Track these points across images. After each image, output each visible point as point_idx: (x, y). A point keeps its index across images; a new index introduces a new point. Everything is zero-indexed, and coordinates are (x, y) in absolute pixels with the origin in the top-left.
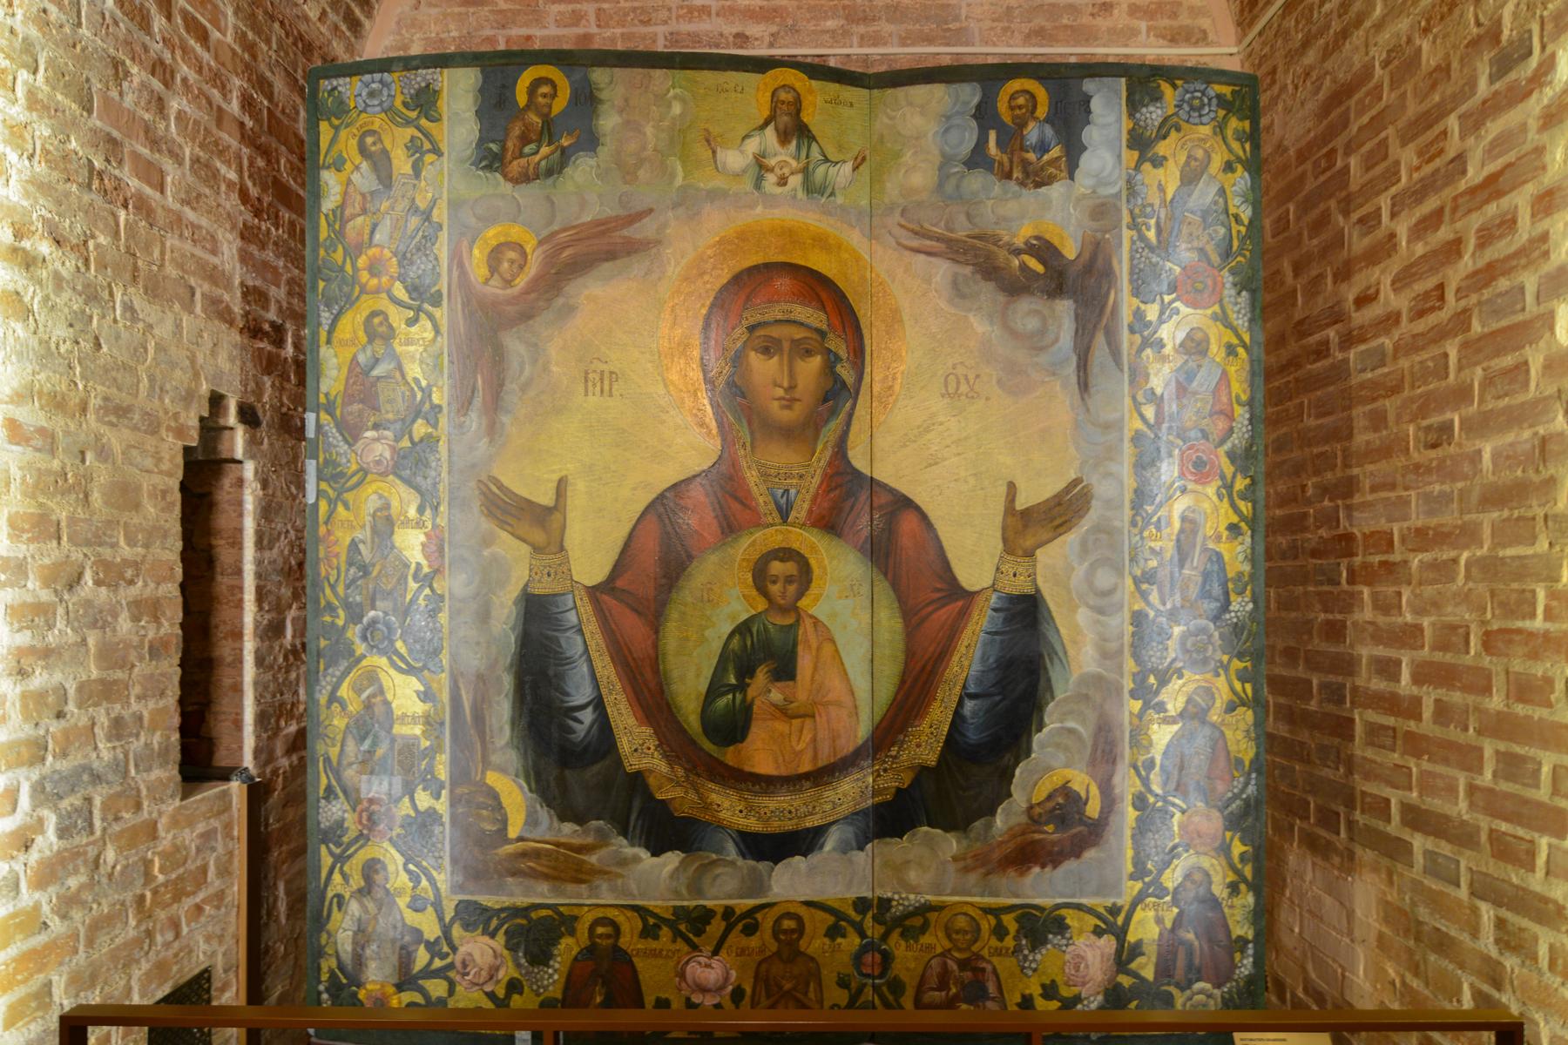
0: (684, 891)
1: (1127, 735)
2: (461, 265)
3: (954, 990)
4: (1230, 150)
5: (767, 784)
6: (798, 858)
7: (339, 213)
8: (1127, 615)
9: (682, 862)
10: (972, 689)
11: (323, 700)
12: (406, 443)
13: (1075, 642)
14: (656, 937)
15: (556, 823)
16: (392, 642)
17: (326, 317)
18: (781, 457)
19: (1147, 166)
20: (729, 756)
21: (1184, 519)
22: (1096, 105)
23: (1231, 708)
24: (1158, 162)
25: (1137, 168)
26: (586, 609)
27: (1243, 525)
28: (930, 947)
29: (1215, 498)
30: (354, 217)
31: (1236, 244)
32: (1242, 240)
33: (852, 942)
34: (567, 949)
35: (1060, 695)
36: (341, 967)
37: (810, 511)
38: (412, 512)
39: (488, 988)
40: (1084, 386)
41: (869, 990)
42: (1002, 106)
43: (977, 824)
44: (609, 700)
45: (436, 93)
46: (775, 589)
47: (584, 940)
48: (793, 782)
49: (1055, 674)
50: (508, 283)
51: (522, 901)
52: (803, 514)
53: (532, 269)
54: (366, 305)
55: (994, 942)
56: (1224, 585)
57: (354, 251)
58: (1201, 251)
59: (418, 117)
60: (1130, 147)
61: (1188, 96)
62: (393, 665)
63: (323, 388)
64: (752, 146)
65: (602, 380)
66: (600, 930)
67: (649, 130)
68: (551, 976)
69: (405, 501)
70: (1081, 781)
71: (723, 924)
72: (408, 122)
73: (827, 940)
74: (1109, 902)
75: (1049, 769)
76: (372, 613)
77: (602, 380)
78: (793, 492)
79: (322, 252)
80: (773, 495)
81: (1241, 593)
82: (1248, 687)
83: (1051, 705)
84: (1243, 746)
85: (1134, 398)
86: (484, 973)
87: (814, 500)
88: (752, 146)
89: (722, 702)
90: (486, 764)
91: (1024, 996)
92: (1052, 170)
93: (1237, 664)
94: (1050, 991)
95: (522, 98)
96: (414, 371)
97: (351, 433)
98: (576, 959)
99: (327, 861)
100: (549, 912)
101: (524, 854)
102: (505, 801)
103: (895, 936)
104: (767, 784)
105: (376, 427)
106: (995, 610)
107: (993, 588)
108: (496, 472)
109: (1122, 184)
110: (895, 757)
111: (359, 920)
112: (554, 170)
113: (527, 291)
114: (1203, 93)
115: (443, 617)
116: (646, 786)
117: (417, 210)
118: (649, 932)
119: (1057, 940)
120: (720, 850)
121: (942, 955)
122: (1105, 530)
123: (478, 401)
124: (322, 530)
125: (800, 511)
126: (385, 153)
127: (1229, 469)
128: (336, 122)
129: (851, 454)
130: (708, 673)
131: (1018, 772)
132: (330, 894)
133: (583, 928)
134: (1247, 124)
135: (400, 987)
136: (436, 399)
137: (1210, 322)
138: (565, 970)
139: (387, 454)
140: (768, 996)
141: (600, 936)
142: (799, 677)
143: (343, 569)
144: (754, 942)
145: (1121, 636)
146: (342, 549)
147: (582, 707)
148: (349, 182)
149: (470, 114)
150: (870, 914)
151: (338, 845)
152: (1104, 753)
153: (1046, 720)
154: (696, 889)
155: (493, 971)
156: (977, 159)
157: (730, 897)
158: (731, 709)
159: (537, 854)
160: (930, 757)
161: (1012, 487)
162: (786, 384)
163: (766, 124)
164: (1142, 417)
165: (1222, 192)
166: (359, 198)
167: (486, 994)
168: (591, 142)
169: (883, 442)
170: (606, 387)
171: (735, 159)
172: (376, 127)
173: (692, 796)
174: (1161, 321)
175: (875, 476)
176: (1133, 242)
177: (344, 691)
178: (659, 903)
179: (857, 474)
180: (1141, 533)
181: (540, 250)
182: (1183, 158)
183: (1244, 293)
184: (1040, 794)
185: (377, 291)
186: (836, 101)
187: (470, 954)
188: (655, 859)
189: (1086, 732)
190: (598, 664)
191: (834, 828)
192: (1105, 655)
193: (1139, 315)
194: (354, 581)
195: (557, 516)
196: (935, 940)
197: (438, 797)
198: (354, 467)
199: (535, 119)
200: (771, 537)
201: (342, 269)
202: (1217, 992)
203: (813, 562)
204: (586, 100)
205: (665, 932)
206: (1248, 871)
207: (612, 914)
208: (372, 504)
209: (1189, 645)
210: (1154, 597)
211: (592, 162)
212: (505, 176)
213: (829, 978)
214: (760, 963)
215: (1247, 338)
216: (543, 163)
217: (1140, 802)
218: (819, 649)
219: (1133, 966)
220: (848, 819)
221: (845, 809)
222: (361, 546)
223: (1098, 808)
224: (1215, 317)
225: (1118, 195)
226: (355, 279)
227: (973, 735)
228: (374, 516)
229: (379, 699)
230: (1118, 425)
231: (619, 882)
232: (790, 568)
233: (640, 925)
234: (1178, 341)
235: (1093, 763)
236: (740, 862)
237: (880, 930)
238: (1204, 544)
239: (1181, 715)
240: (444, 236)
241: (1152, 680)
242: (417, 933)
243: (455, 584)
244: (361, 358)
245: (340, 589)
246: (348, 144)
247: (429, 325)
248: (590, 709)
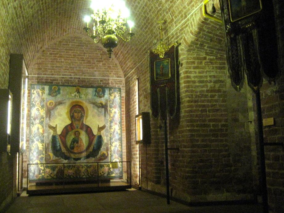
5: (75, 153)
8: (109, 137)
11: (31, 146)
16: (39, 140)
18: (77, 122)
20: (72, 151)
22: (106, 91)
23: (119, 146)
24: (112, 96)
26: (59, 137)
32: (120, 103)
33: (84, 169)
34: (57, 169)
38: (41, 128)
40: (105, 116)
44: (61, 145)
47: (58, 168)
49: (103, 143)
50: (51, 106)
53: (54, 105)
54: (36, 107)
57: (35, 102)
60: (109, 94)
63: (32, 115)
64: (75, 94)
67: (65, 92)
69: (40, 126)
70: (105, 152)
72: (41, 90)
88: (75, 94)
90: (49, 152)
93: (119, 142)
94: (103, 172)
96: (41, 114)
97: (35, 119)
102: (51, 156)
104: (75, 153)
107: (97, 135)
108: (50, 124)
112: (56, 95)
113: (53, 107)
115: (44, 138)
122: (107, 129)
123: (48, 117)
125: (79, 128)
130: (70, 143)
135: (39, 175)
136: (44, 116)
144: (75, 169)
152: (107, 150)
155: (49, 172)
156: (95, 95)
161: (99, 126)
168: (59, 93)
171: (73, 95)
177: (33, 145)
179: (84, 124)
184: (102, 153)
188: (65, 161)
189: (105, 148)
192: (107, 141)
193: (110, 110)
196: (92, 168)
197: (43, 155)
200: (77, 130)
204: (59, 89)
205: (66, 168)
210: (112, 136)
212: (52, 96)
213: (82, 172)
217: (111, 154)
220: (84, 157)
230: (108, 120)
232: (78, 133)
239: (114, 146)
240: (45, 101)
242: (41, 169)
243: (46, 134)
246: (35, 92)
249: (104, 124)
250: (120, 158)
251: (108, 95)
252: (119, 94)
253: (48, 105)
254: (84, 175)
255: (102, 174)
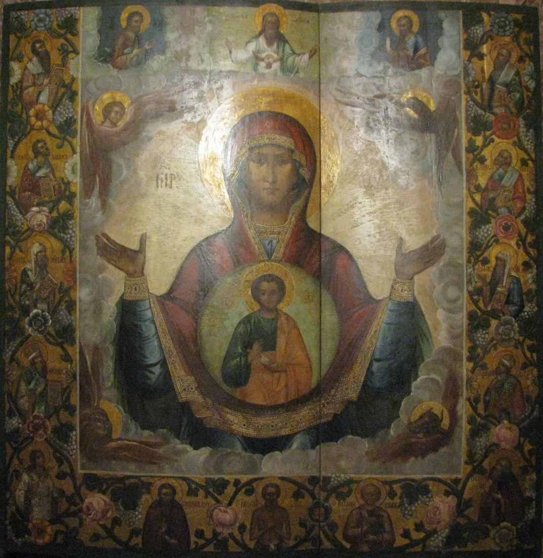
0: (211, 469)
1: (464, 383)
2: (88, 114)
3: (365, 528)
4: (522, 50)
5: (259, 410)
6: (277, 453)
7: (20, 85)
9: (211, 454)
10: (377, 356)
12: (55, 214)
13: (436, 329)
14: (196, 495)
15: (139, 430)
17: (11, 143)
19: (475, 60)
20: (237, 393)
21: (497, 258)
22: (445, 25)
23: (525, 366)
25: (469, 60)
26: (156, 309)
27: (531, 262)
28: (352, 504)
29: (515, 247)
30: (27, 87)
31: (526, 102)
33: (307, 501)
34: (146, 500)
35: (427, 360)
36: (18, 509)
37: (284, 253)
39: (101, 522)
41: (317, 528)
42: (394, 25)
43: (380, 433)
45: (76, 20)
46: (264, 298)
47: (156, 497)
48: (274, 409)
49: (424, 347)
50: (114, 124)
51: (120, 474)
52: (280, 255)
54: (35, 136)
55: (388, 500)
56: (521, 294)
58: (507, 106)
59: (66, 33)
60: (465, 48)
61: (497, 20)
62: (48, 341)
64: (252, 47)
65: (166, 179)
66: (164, 491)
68: (137, 516)
70: (438, 407)
71: (234, 489)
73: (293, 499)
74: (454, 476)
75: (420, 401)
76: (35, 311)
77: (166, 179)
78: (274, 242)
79: (9, 107)
80: (263, 244)
81: (530, 302)
82: (534, 355)
83: (422, 365)
84: (531, 388)
85: (469, 189)
86: (99, 514)
87: (286, 247)
88: (252, 47)
89: (234, 362)
91: (404, 530)
92: (422, 61)
93: (528, 342)
95: (124, 24)
97: (24, 209)
98: (151, 507)
99: (9, 450)
100: (136, 481)
101: (120, 448)
103: (332, 498)
104: (259, 410)
105: (38, 205)
106: (391, 311)
107: (390, 298)
108: (107, 232)
109: (460, 69)
110: (334, 396)
111: (28, 484)
114: (506, 18)
116: (189, 409)
117: (64, 86)
118: (192, 492)
119: (425, 498)
120: (232, 446)
121: (359, 508)
124: (7, 263)
125: (279, 254)
126: (47, 54)
127: (523, 230)
128: (19, 35)
129: (308, 220)
130: (225, 347)
131: (403, 404)
132: (11, 470)
133: (155, 490)
134: (531, 35)
137: (511, 147)
138: (145, 513)
139: (45, 220)
140: (260, 529)
141: (165, 494)
142: (277, 349)
143: (18, 286)
145: (462, 327)
146: (18, 275)
147: (154, 365)
148: (26, 68)
149: (95, 32)
150: (318, 486)
151: (15, 443)
153: (419, 373)
154: (218, 469)
155: (105, 512)
157: (239, 473)
158: (238, 366)
159: (128, 448)
160: (353, 395)
162: (270, 180)
163: (260, 34)
164: (473, 199)
165: (517, 74)
166: (31, 76)
167: (101, 525)
169: (327, 212)
170: (169, 182)
172: (42, 38)
173: (217, 416)
174: (485, 146)
175: (323, 232)
176: (467, 102)
178: (198, 476)
180: (473, 266)
181: (132, 107)
182: (495, 54)
183: (531, 130)
184: (415, 416)
185: (42, 128)
186: (300, 20)
187: (91, 503)
188: (196, 451)
190: (163, 341)
191: (298, 436)
194: (25, 292)
195: (141, 256)
196: (354, 499)
198: (26, 228)
199: (131, 35)
201: (20, 116)
202: (514, 528)
203: (286, 283)
205: (201, 493)
206: (534, 460)
207: (173, 482)
208: (36, 248)
209: (500, 331)
211: (163, 58)
214: (255, 511)
215: (533, 156)
216: (135, 58)
218: (289, 333)
219: (466, 513)
220: (307, 431)
221: (303, 425)
222: (29, 273)
223: (448, 424)
224: (514, 144)
225: (458, 76)
226: (28, 122)
227: (377, 383)
228: (36, 255)
229: (39, 359)
231: (176, 464)
232: (273, 285)
233: (187, 488)
234: (494, 157)
235: (445, 398)
236: (244, 454)
237: (323, 495)
238: (509, 273)
240: (79, 98)
241: (479, 350)
244: (31, 166)
245: (17, 297)
247: (69, 147)
248: (158, 366)
249: (434, 233)
250: (531, 443)
251: (459, 53)
252: (528, 43)
253: (97, 118)
254: (305, 540)
255: (417, 536)
